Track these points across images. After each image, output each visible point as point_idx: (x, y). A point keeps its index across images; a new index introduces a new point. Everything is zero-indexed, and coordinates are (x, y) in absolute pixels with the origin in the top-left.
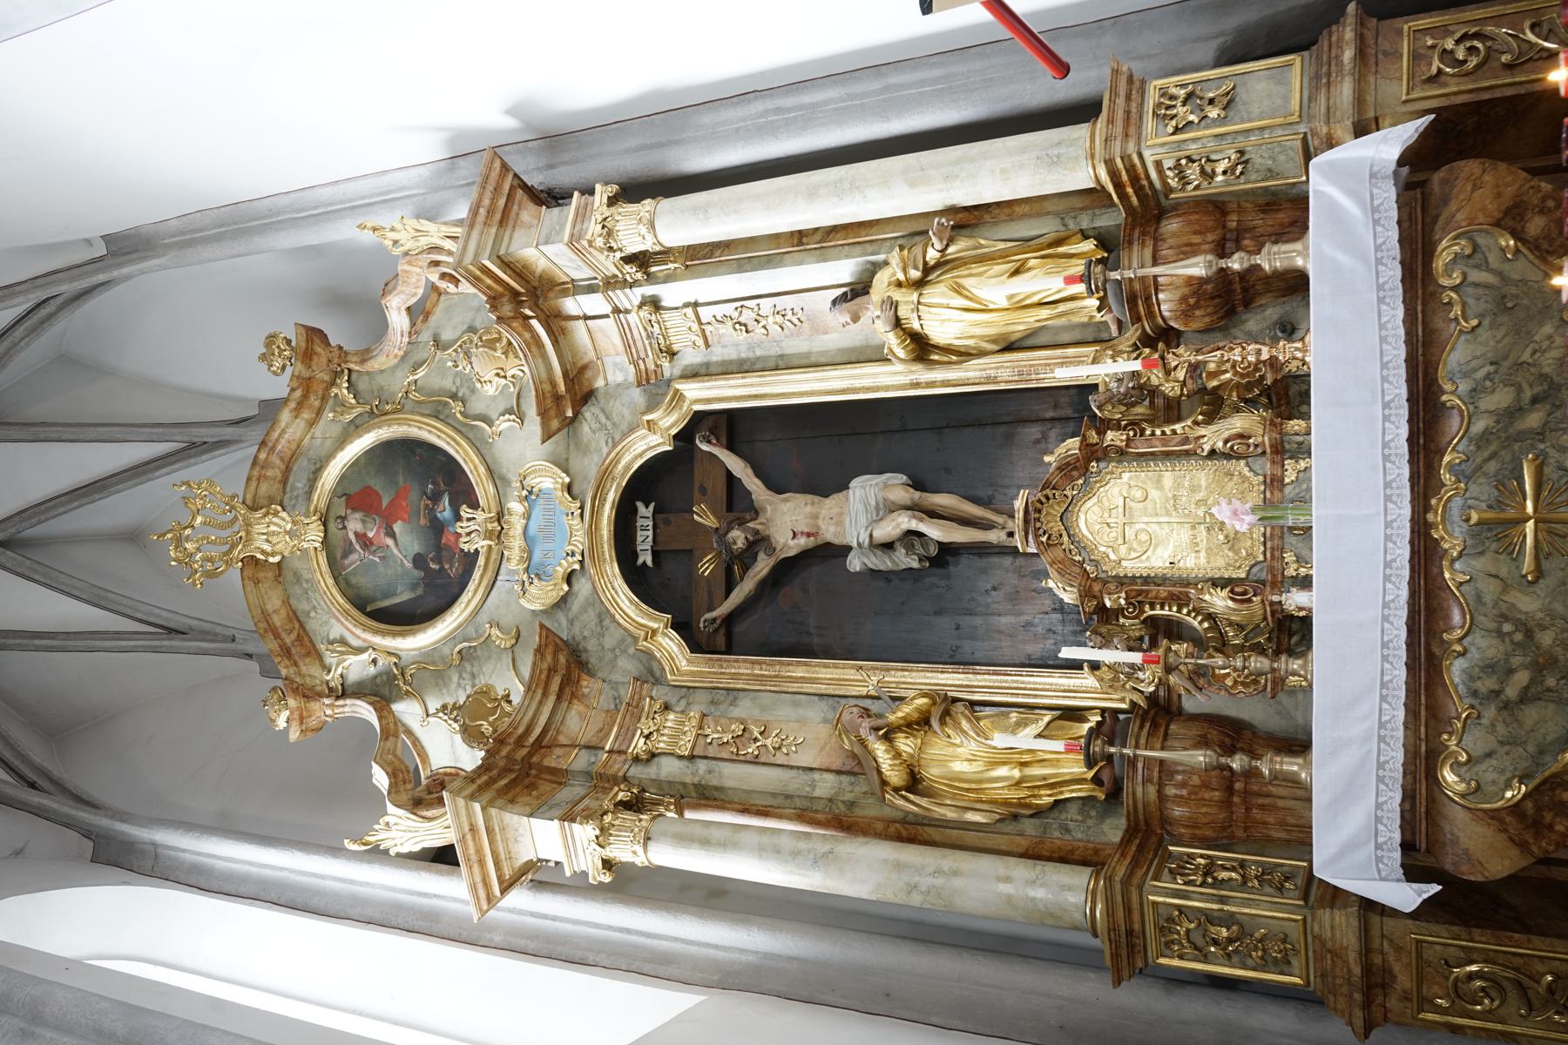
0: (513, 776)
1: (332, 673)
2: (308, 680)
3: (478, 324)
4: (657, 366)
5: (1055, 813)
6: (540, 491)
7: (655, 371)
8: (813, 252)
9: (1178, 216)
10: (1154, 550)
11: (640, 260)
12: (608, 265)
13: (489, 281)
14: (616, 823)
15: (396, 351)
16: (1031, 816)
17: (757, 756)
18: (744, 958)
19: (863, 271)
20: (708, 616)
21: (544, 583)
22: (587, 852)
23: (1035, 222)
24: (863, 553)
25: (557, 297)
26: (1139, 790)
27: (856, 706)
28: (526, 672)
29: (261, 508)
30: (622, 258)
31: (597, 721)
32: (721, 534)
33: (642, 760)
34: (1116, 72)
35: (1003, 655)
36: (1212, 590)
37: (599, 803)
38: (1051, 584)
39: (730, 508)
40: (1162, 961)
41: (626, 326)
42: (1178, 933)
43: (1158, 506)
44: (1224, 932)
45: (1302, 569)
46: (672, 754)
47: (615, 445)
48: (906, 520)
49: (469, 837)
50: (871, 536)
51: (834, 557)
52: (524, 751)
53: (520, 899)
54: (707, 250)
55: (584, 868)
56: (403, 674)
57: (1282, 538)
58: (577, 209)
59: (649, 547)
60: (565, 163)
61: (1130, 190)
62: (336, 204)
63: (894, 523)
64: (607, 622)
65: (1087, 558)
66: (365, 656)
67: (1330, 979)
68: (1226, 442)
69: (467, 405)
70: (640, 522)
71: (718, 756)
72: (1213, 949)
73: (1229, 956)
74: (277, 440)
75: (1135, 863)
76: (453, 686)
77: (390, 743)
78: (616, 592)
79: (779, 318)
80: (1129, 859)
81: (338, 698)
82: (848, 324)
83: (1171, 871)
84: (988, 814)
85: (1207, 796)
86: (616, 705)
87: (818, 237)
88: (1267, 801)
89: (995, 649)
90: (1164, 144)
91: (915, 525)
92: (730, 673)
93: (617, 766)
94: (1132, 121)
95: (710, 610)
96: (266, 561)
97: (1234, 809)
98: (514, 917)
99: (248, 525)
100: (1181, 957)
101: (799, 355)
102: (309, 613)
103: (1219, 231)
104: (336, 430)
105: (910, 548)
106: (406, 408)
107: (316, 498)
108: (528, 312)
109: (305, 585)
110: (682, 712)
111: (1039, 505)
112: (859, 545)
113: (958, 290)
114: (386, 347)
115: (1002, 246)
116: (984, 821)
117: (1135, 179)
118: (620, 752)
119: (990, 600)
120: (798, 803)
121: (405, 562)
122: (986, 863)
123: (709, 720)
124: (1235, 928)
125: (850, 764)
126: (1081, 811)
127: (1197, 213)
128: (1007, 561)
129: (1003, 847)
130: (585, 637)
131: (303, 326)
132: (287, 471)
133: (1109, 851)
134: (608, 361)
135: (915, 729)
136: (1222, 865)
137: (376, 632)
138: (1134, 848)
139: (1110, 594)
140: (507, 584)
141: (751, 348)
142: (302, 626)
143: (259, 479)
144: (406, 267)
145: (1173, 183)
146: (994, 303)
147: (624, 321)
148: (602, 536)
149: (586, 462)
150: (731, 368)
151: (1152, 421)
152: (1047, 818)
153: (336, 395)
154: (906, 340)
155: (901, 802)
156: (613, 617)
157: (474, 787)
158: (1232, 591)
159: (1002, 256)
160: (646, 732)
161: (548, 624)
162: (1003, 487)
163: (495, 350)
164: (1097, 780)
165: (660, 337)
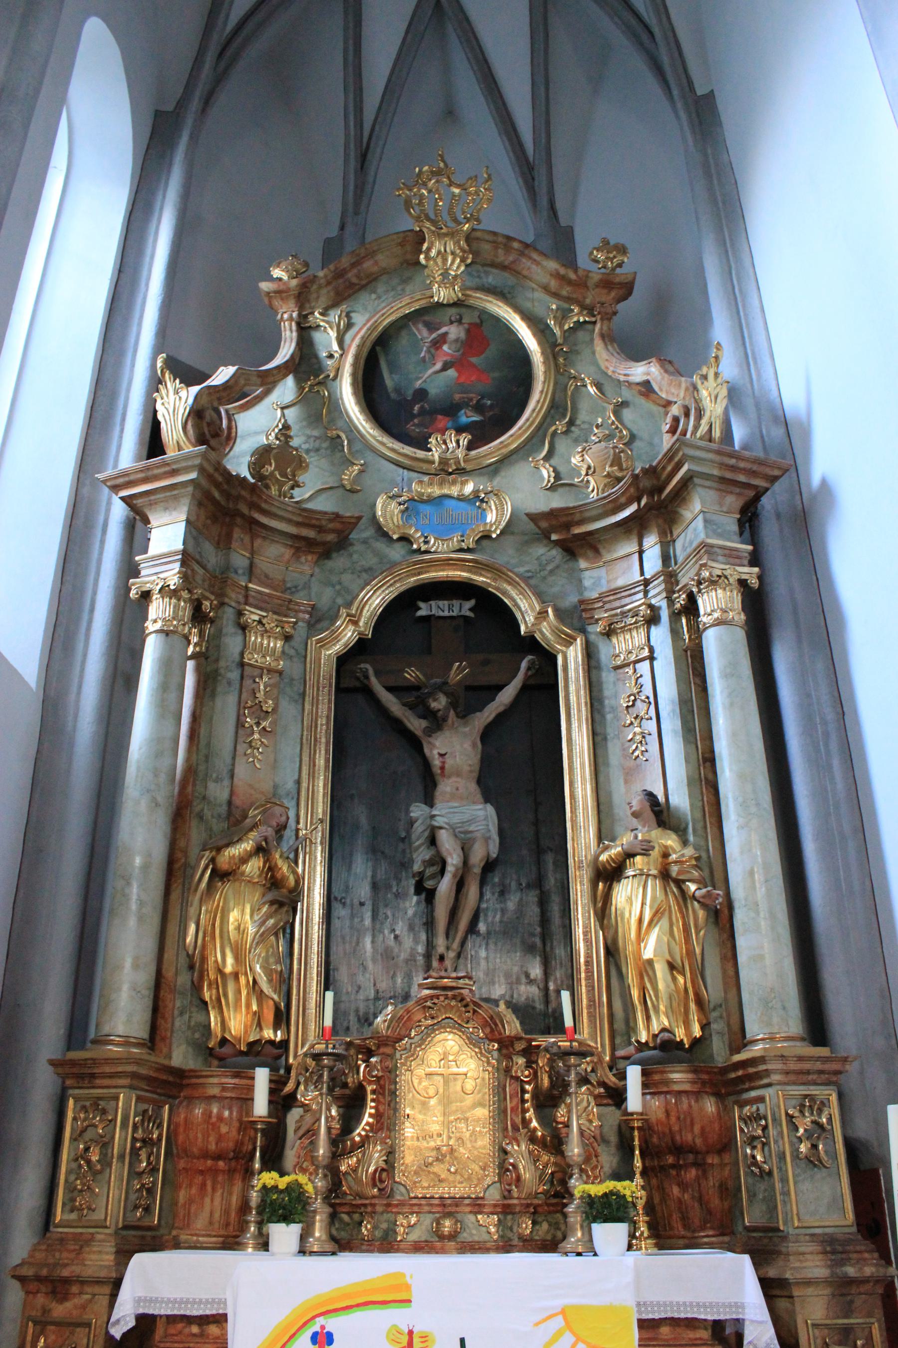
0: (223, 503)
1: (321, 317)
2: (314, 296)
3: (637, 444)
4: (597, 620)
5: (196, 1002)
6: (484, 510)
7: (593, 617)
8: (697, 772)
9: (719, 1113)
10: (420, 1100)
11: (691, 608)
12: (686, 578)
13: (669, 468)
14: (182, 604)
15: (611, 369)
16: (193, 982)
17: (244, 726)
18: (70, 718)
19: (679, 819)
20: (371, 672)
21: (400, 516)
22: (155, 577)
23: (720, 981)
24: (426, 819)
25: (658, 526)
26: (215, 1080)
27: (288, 818)
28: (316, 505)
29: (468, 245)
30: (692, 592)
31: (275, 571)
32: (442, 687)
33: (239, 619)
34: (845, 1060)
35: (337, 946)
36: (384, 1152)
37: (200, 582)
38: (390, 1008)
39: (469, 688)
40: (71, 1102)
41: (633, 591)
42: (94, 1118)
43: (458, 1104)
44: (95, 1158)
45: (402, 1229)
46: (245, 646)
47: (526, 579)
48: (454, 862)
49: (167, 469)
50: (441, 828)
51: (426, 787)
52: (245, 510)
53: (118, 511)
54: (700, 669)
55: (143, 573)
56: (319, 383)
57: (430, 1212)
58: (736, 550)
59: (433, 612)
60: (781, 531)
61: (740, 1073)
62: (744, 310)
63: (452, 851)
64: (364, 575)
65: (412, 1041)
66: (335, 347)
67: (58, 1247)
68: (512, 1164)
69: (563, 436)
70: (456, 603)
71: (244, 690)
72: (81, 1146)
73: (76, 1160)
74: (530, 258)
75: (149, 1079)
76: (308, 432)
77: (255, 379)
78: (391, 585)
79: (638, 738)
80: (152, 1073)
81: (298, 324)
82: (631, 807)
83: (145, 1112)
84: (193, 944)
85: (211, 1139)
86: (289, 588)
87: (710, 776)
88: (209, 1188)
89: (343, 938)
90: (779, 1107)
91: (450, 869)
92: (318, 695)
93: (233, 595)
94: (801, 1076)
95: (377, 674)
96: (421, 252)
97: (202, 1160)
98: (104, 503)
99: (452, 235)
100: (75, 1119)
101: (606, 756)
102: (374, 292)
103: (704, 1149)
104: (539, 311)
105: (430, 863)
106: (559, 377)
107: (478, 295)
108: (643, 502)
109: (399, 288)
110: (283, 652)
111: (459, 999)
112: (434, 816)
113: (657, 914)
114: (614, 360)
115: (698, 950)
116: (188, 940)
117: (751, 1078)
118: (246, 597)
119: (386, 932)
120: (202, 768)
121: (420, 382)
122: (150, 945)
123: (276, 678)
124: (99, 1167)
125: (237, 814)
126: (198, 1025)
127: (720, 1129)
128: (421, 949)
129: (166, 956)
130: (351, 555)
131: (634, 279)
132: (504, 267)
133: (165, 1050)
134: (602, 572)
135: (267, 875)
136: (152, 1153)
137: (357, 357)
138: (164, 1077)
139: (381, 1061)
140: (400, 478)
141: (614, 709)
142: (363, 287)
143: (494, 242)
144: (683, 385)
145: (747, 1110)
146: (645, 948)
147: (637, 589)
148: (443, 570)
149: (511, 552)
150: (594, 689)
151: (536, 1088)
152: (192, 995)
153: (572, 310)
154: (614, 862)
155: (203, 863)
156: (368, 584)
157: (211, 470)
158: (383, 1170)
159: (690, 953)
160: (264, 621)
161: (363, 521)
162: (487, 944)
163: (611, 466)
164: (224, 1041)
165: (623, 624)
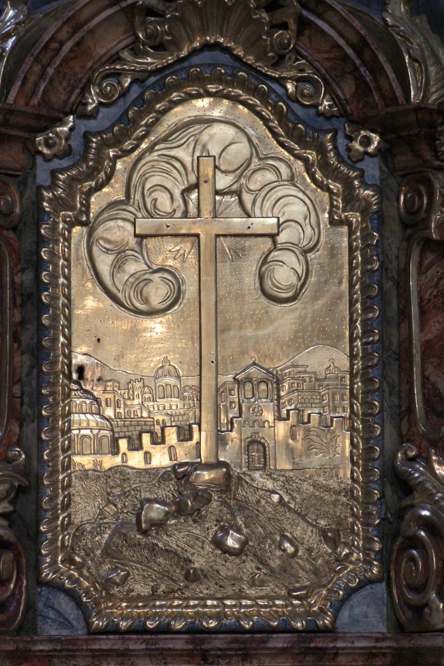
65: (92, 125)
